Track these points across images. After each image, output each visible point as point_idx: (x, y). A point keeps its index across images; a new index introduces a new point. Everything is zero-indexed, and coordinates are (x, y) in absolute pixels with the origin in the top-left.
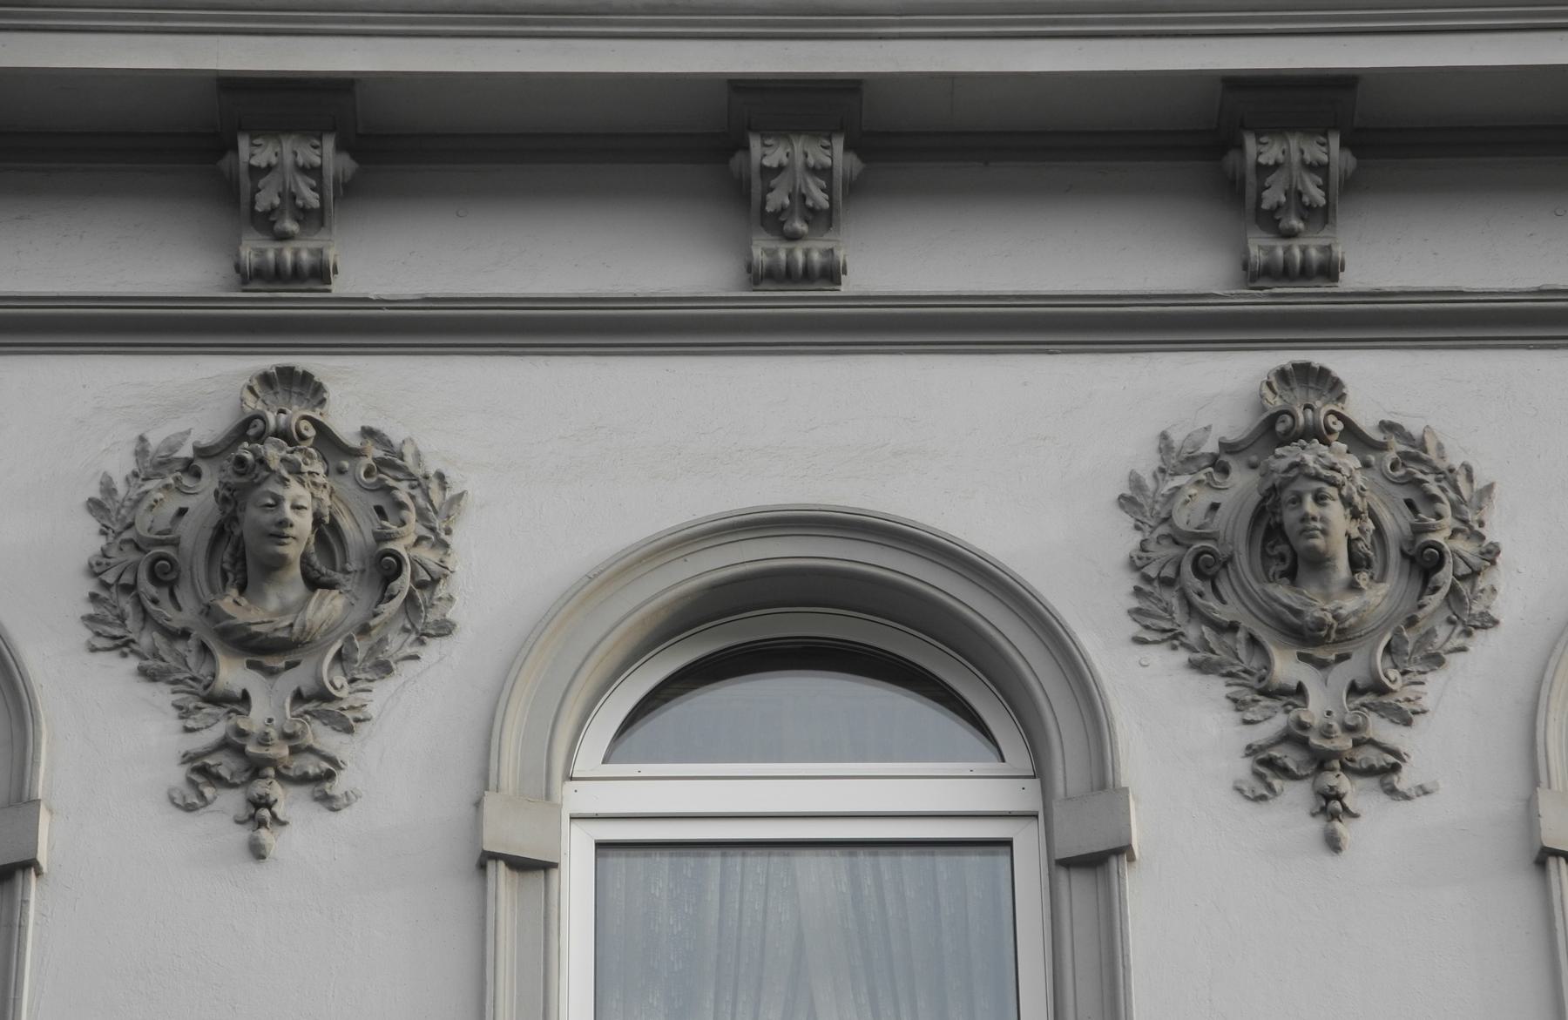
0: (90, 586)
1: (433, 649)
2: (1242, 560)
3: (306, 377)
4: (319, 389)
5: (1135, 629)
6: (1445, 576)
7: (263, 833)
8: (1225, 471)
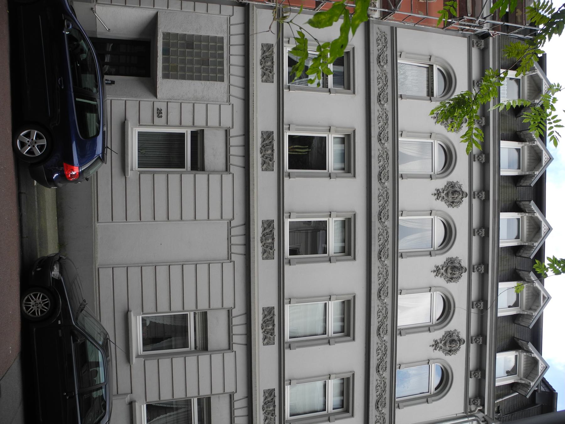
2: (451, 338)
5: (446, 331)
6: (449, 353)
7: (433, 272)
8: (457, 337)
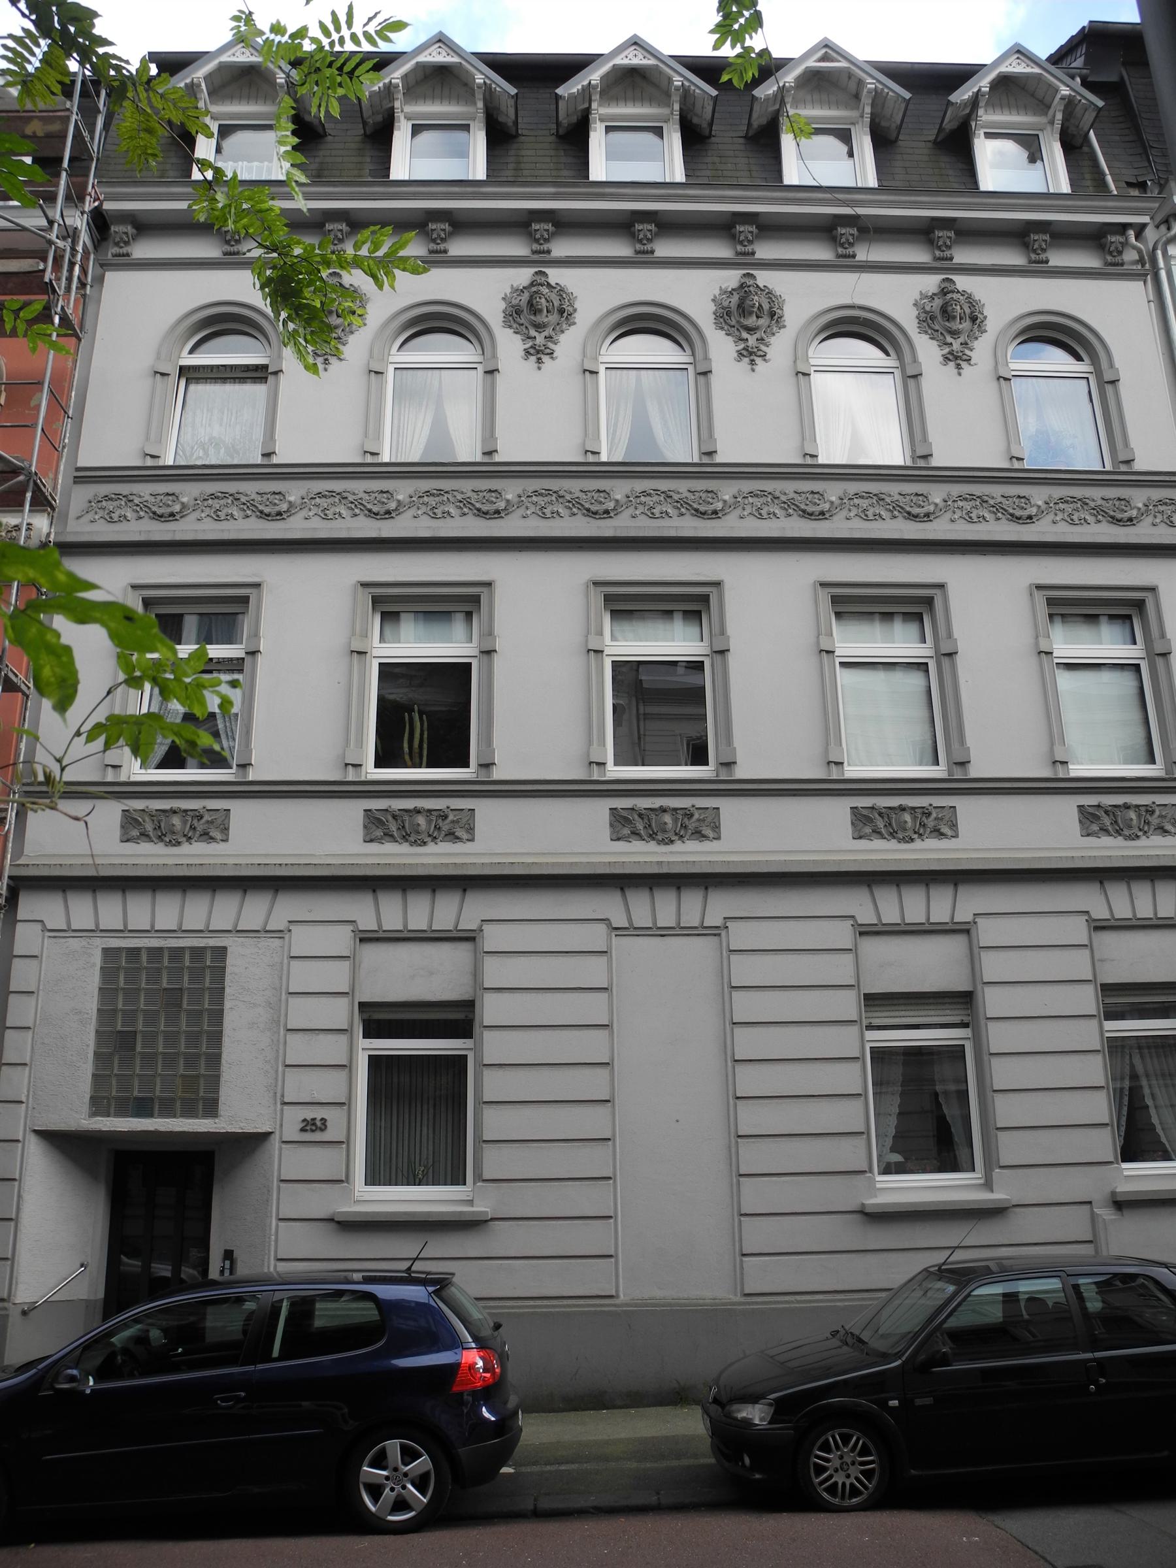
0: (714, 316)
1: (782, 330)
2: (939, 317)
3: (752, 275)
4: (755, 277)
5: (918, 330)
6: (978, 322)
7: (754, 367)
8: (933, 299)
